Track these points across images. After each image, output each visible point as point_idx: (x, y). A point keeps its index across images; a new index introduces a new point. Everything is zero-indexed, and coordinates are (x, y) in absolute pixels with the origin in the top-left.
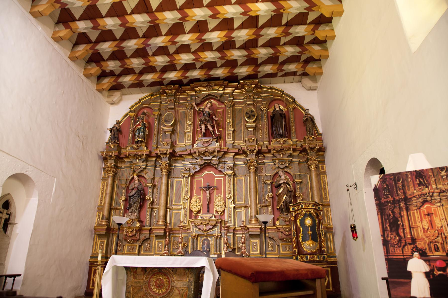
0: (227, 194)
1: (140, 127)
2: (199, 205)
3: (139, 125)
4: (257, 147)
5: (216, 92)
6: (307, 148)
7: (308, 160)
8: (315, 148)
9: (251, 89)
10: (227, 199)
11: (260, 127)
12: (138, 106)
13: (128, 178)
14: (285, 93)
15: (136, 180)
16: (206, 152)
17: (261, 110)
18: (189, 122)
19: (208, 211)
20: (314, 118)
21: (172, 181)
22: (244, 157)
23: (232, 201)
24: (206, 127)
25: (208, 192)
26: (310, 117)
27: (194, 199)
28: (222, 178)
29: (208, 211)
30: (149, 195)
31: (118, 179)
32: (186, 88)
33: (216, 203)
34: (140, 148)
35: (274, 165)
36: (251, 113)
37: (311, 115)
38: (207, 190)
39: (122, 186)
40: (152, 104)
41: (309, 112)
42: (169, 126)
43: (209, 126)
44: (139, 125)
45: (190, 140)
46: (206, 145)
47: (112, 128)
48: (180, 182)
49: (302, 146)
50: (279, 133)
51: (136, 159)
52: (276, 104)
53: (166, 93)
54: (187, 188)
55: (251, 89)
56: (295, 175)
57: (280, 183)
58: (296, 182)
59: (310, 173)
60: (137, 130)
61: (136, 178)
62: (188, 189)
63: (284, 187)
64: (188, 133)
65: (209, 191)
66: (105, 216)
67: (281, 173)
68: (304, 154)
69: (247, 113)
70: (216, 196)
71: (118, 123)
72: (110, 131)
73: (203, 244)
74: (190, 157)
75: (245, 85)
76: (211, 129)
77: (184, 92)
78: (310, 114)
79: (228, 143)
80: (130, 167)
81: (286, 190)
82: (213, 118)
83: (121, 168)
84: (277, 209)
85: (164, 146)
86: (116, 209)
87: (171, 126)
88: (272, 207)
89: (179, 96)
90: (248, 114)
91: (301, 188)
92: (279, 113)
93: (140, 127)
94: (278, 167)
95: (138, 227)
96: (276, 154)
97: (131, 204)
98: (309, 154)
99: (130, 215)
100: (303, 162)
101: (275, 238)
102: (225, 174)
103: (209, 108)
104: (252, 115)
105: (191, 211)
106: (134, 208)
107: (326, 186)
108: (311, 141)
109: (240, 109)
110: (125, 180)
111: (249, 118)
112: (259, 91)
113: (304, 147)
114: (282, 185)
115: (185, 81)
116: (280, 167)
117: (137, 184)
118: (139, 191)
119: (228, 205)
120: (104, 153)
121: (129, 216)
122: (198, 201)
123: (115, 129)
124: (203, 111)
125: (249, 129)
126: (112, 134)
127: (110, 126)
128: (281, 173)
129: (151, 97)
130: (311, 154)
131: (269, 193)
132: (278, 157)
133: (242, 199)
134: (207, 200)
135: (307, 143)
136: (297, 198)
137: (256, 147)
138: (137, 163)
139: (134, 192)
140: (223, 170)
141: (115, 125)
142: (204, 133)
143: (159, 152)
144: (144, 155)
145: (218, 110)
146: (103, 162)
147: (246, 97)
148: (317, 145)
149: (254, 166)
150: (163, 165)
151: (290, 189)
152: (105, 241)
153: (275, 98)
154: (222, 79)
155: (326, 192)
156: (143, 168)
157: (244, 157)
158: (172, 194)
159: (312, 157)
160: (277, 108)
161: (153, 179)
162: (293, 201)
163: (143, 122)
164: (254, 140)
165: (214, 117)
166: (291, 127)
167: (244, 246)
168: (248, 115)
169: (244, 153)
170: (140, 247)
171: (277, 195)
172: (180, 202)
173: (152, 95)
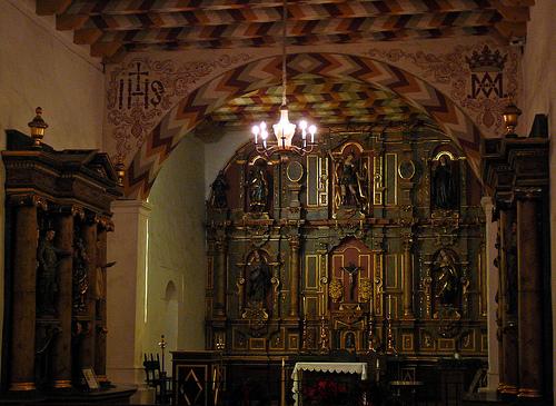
19: (352, 297)
24: (347, 189)
27: (334, 282)
29: (352, 297)
43: (350, 187)
46: (349, 216)
73: (347, 339)
91: (468, 272)
105: (330, 298)
106: (258, 294)
139: (256, 275)
161: (279, 257)
170: (268, 341)
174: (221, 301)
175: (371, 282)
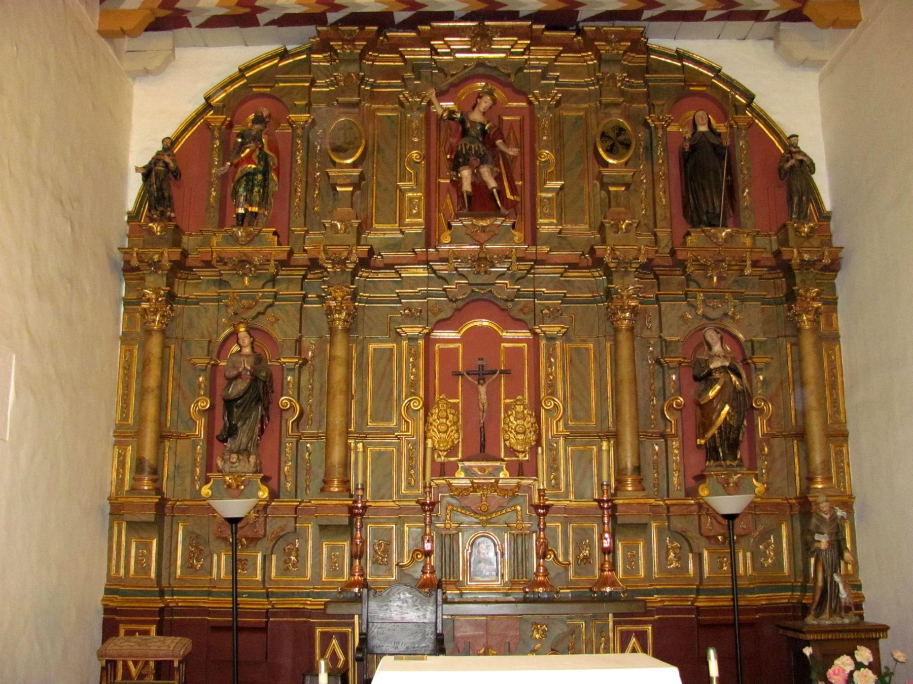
0: (542, 395)
1: (253, 166)
2: (453, 428)
3: (249, 159)
4: (643, 252)
5: (503, 55)
6: (795, 262)
7: (791, 297)
8: (820, 260)
9: (618, 54)
10: (543, 412)
11: (642, 181)
12: (235, 90)
13: (215, 336)
14: (724, 74)
15: (245, 347)
16: (479, 259)
17: (646, 125)
18: (414, 154)
19: (483, 447)
20: (813, 164)
21: (359, 347)
22: (594, 277)
23: (559, 420)
24: (476, 175)
25: (483, 389)
26: (802, 161)
28: (526, 345)
29: (483, 447)
30: (288, 395)
31: (177, 338)
32: (400, 38)
33: (510, 424)
34: (256, 239)
35: (687, 308)
36: (618, 135)
37: (805, 155)
38: (482, 382)
39: (194, 364)
40: (281, 84)
41: (799, 145)
42: (348, 166)
44: (249, 159)
45: (417, 215)
47: (150, 163)
48: (388, 353)
49: (777, 254)
50: (711, 208)
51: (245, 275)
52: (701, 113)
53: (332, 49)
54: (412, 374)
55: (618, 54)
56: (751, 341)
57: (712, 366)
58: (754, 363)
59: (797, 336)
60: (242, 177)
61: (245, 338)
62: (416, 375)
63: (722, 381)
64: (411, 190)
65: (485, 386)
66: (147, 464)
67: (712, 336)
68: (775, 276)
69: (603, 135)
70: (508, 401)
71: (169, 145)
72: (143, 174)
74: (421, 272)
75: (598, 41)
76: (492, 184)
77: (394, 47)
78: (803, 149)
79: (544, 229)
80: (219, 301)
81: (729, 390)
82: (494, 146)
83: (186, 301)
84: (699, 446)
85: (337, 232)
86: (179, 437)
87: (354, 165)
88: (681, 439)
89: (374, 61)
90: (609, 137)
92: (709, 142)
93: (253, 166)
94: (704, 316)
95: (263, 500)
96: (698, 274)
97: (236, 425)
98: (798, 279)
99: (234, 460)
100: (776, 302)
101: (689, 534)
102: (538, 331)
103: (484, 114)
104: (622, 143)
106: (242, 438)
107: (837, 378)
108: (802, 240)
109: (578, 118)
110: (206, 344)
111: (610, 151)
112: (638, 59)
113: (785, 257)
114: (717, 375)
115: (400, 16)
116: (708, 315)
117: (251, 360)
118: (255, 379)
119: (547, 431)
120: (135, 255)
121: (233, 463)
122: (451, 416)
123: (160, 168)
124: (462, 121)
125: (612, 189)
126: (151, 185)
127: (145, 160)
128: (712, 336)
129: (279, 62)
130: (803, 281)
131: (673, 395)
132: (705, 283)
133: (588, 411)
134: (481, 414)
135: (791, 243)
136: (756, 412)
137: (640, 250)
138: (246, 288)
139: (241, 386)
140: (528, 318)
141: (158, 153)
142: (469, 197)
143: (322, 254)
144: (272, 262)
145: (505, 118)
146: (121, 280)
147: (598, 79)
148: (826, 253)
149: (633, 310)
150: (335, 299)
151: (739, 387)
152: (155, 542)
153: (691, 88)
154: (526, 14)
155: (837, 395)
156: (267, 304)
157: (594, 277)
158: (364, 391)
159: (807, 291)
160: (703, 125)
162: (745, 423)
163: (261, 149)
164: (631, 224)
165: (499, 142)
166: (741, 189)
167: (609, 561)
168: (609, 143)
169: (598, 262)
171: (702, 403)
172: (390, 419)
173: (284, 55)
174: (148, 454)
175: (536, 405)
